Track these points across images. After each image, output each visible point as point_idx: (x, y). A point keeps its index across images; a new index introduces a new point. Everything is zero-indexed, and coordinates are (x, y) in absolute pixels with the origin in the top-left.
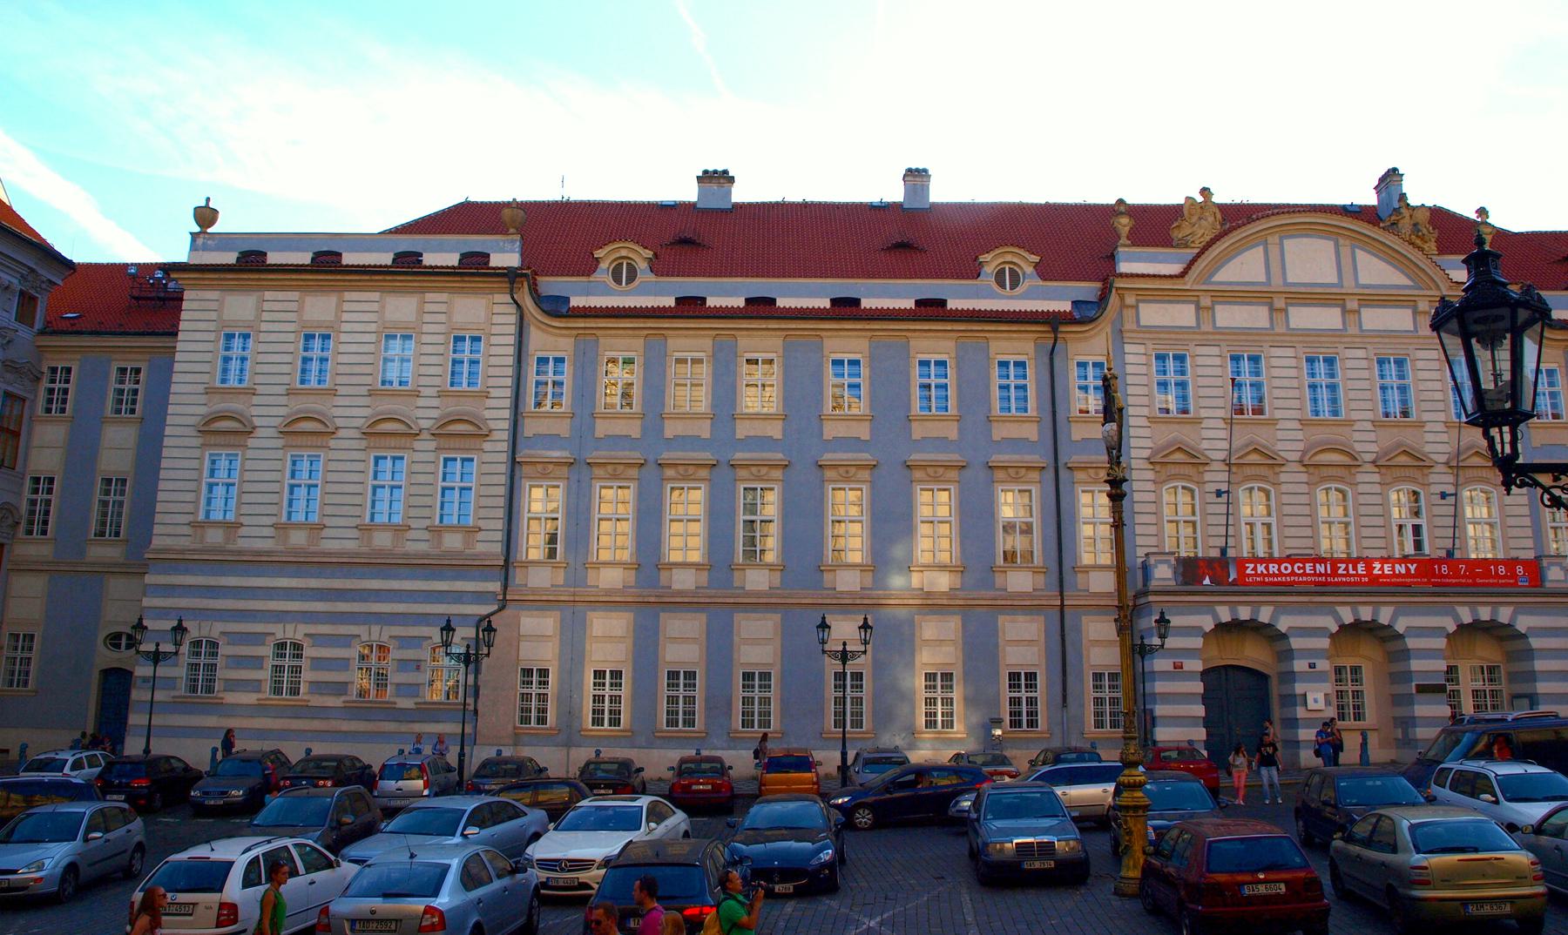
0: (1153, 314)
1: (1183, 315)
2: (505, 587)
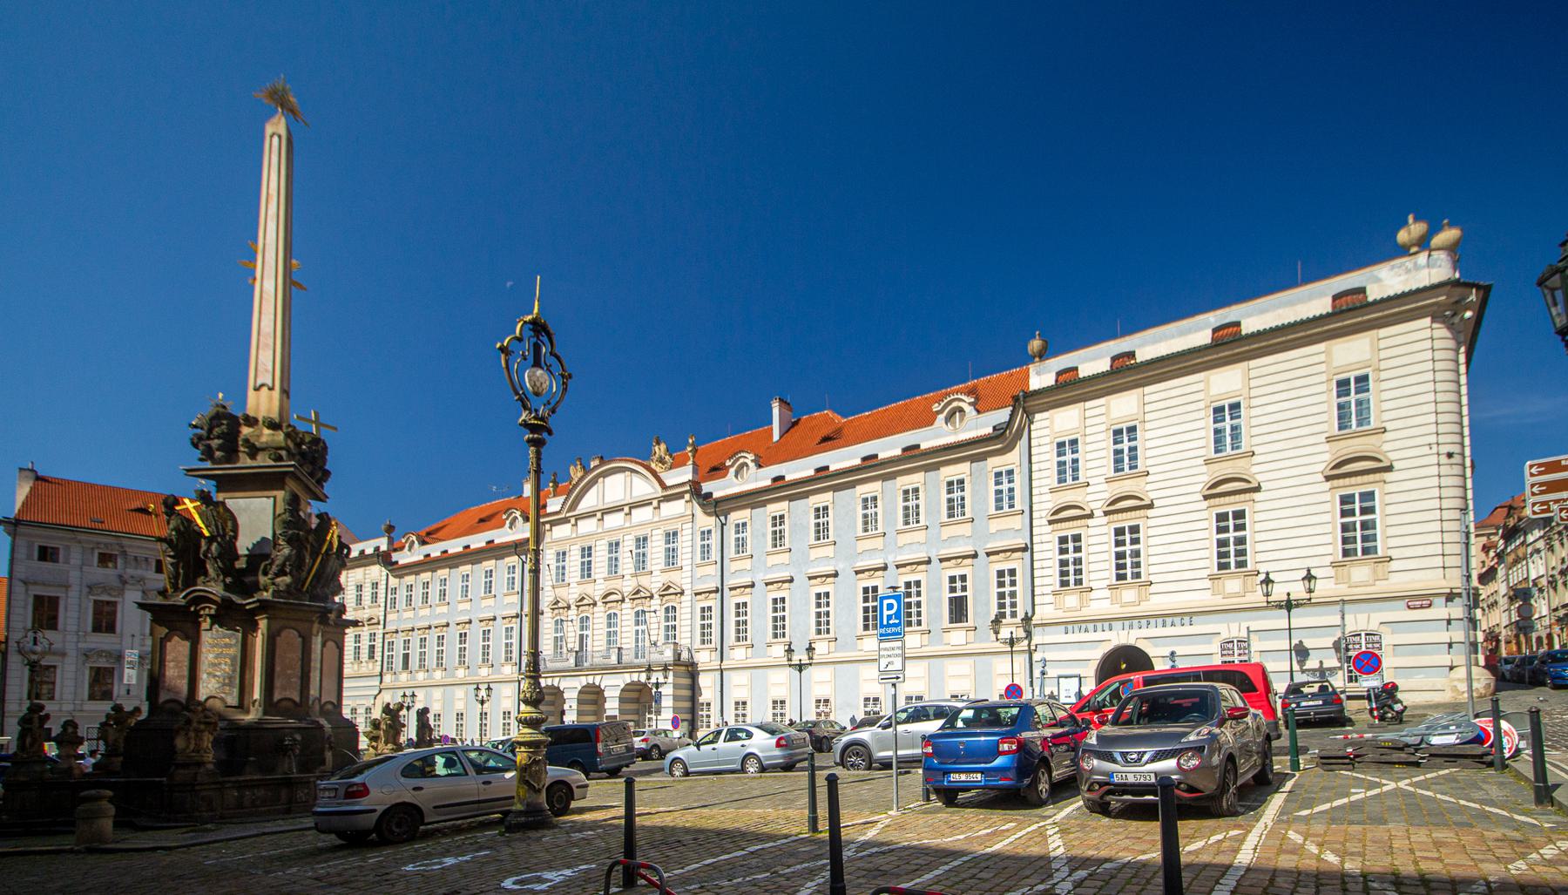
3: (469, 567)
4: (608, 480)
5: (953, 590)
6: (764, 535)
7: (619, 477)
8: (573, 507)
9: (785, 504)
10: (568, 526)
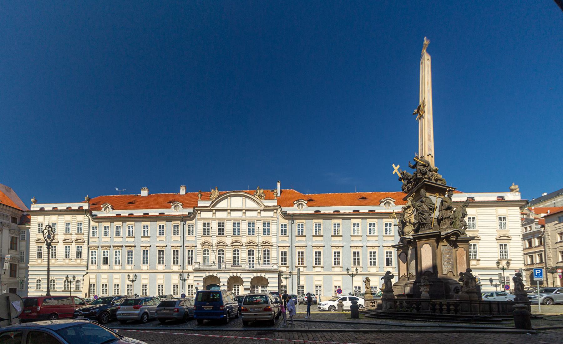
0: (204, 214)
1: (209, 214)
2: (87, 269)
3: (149, 223)
4: (233, 198)
5: (387, 256)
6: (311, 230)
7: (239, 199)
8: (214, 206)
9: (321, 221)
10: (211, 213)
